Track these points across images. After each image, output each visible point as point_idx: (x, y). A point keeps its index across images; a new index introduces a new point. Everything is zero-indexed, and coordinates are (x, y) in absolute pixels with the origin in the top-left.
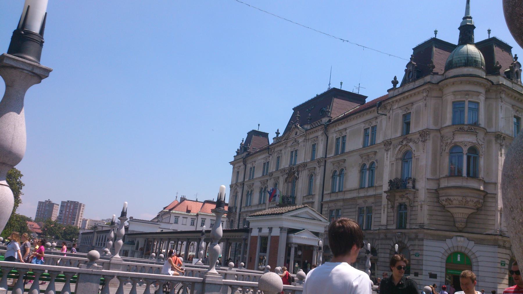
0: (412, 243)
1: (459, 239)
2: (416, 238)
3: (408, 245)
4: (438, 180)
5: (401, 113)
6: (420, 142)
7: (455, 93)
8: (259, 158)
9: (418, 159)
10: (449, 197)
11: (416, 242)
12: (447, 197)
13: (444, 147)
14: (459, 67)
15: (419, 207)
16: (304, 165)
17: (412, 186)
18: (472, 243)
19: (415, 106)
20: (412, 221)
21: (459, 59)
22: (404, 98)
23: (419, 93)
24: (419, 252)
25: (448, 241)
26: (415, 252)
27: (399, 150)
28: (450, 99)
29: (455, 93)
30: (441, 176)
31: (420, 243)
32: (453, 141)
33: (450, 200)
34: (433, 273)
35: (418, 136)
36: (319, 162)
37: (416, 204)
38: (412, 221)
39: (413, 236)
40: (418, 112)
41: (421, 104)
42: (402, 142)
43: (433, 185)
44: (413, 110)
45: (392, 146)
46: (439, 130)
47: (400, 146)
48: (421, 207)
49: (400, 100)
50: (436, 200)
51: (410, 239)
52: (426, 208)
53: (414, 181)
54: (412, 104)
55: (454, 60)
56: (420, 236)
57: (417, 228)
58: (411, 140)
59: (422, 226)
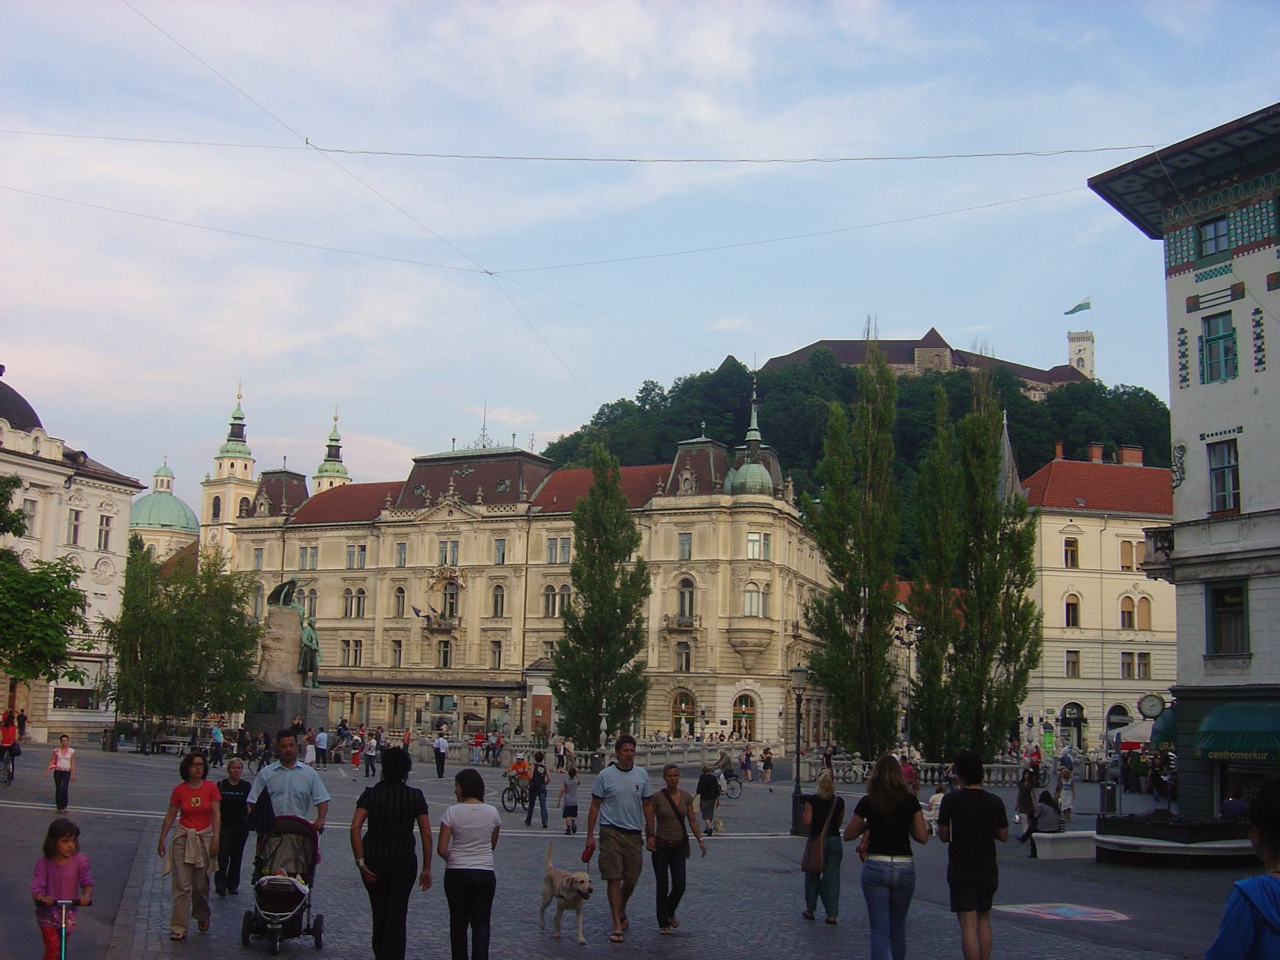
0: (699, 688)
5: (676, 531)
8: (329, 534)
11: (706, 688)
16: (479, 569)
19: (697, 527)
31: (712, 688)
36: (516, 568)
39: (700, 680)
40: (702, 536)
43: (724, 625)
44: (695, 531)
45: (661, 570)
46: (731, 562)
51: (697, 684)
54: (693, 523)
58: (693, 568)
59: (714, 670)
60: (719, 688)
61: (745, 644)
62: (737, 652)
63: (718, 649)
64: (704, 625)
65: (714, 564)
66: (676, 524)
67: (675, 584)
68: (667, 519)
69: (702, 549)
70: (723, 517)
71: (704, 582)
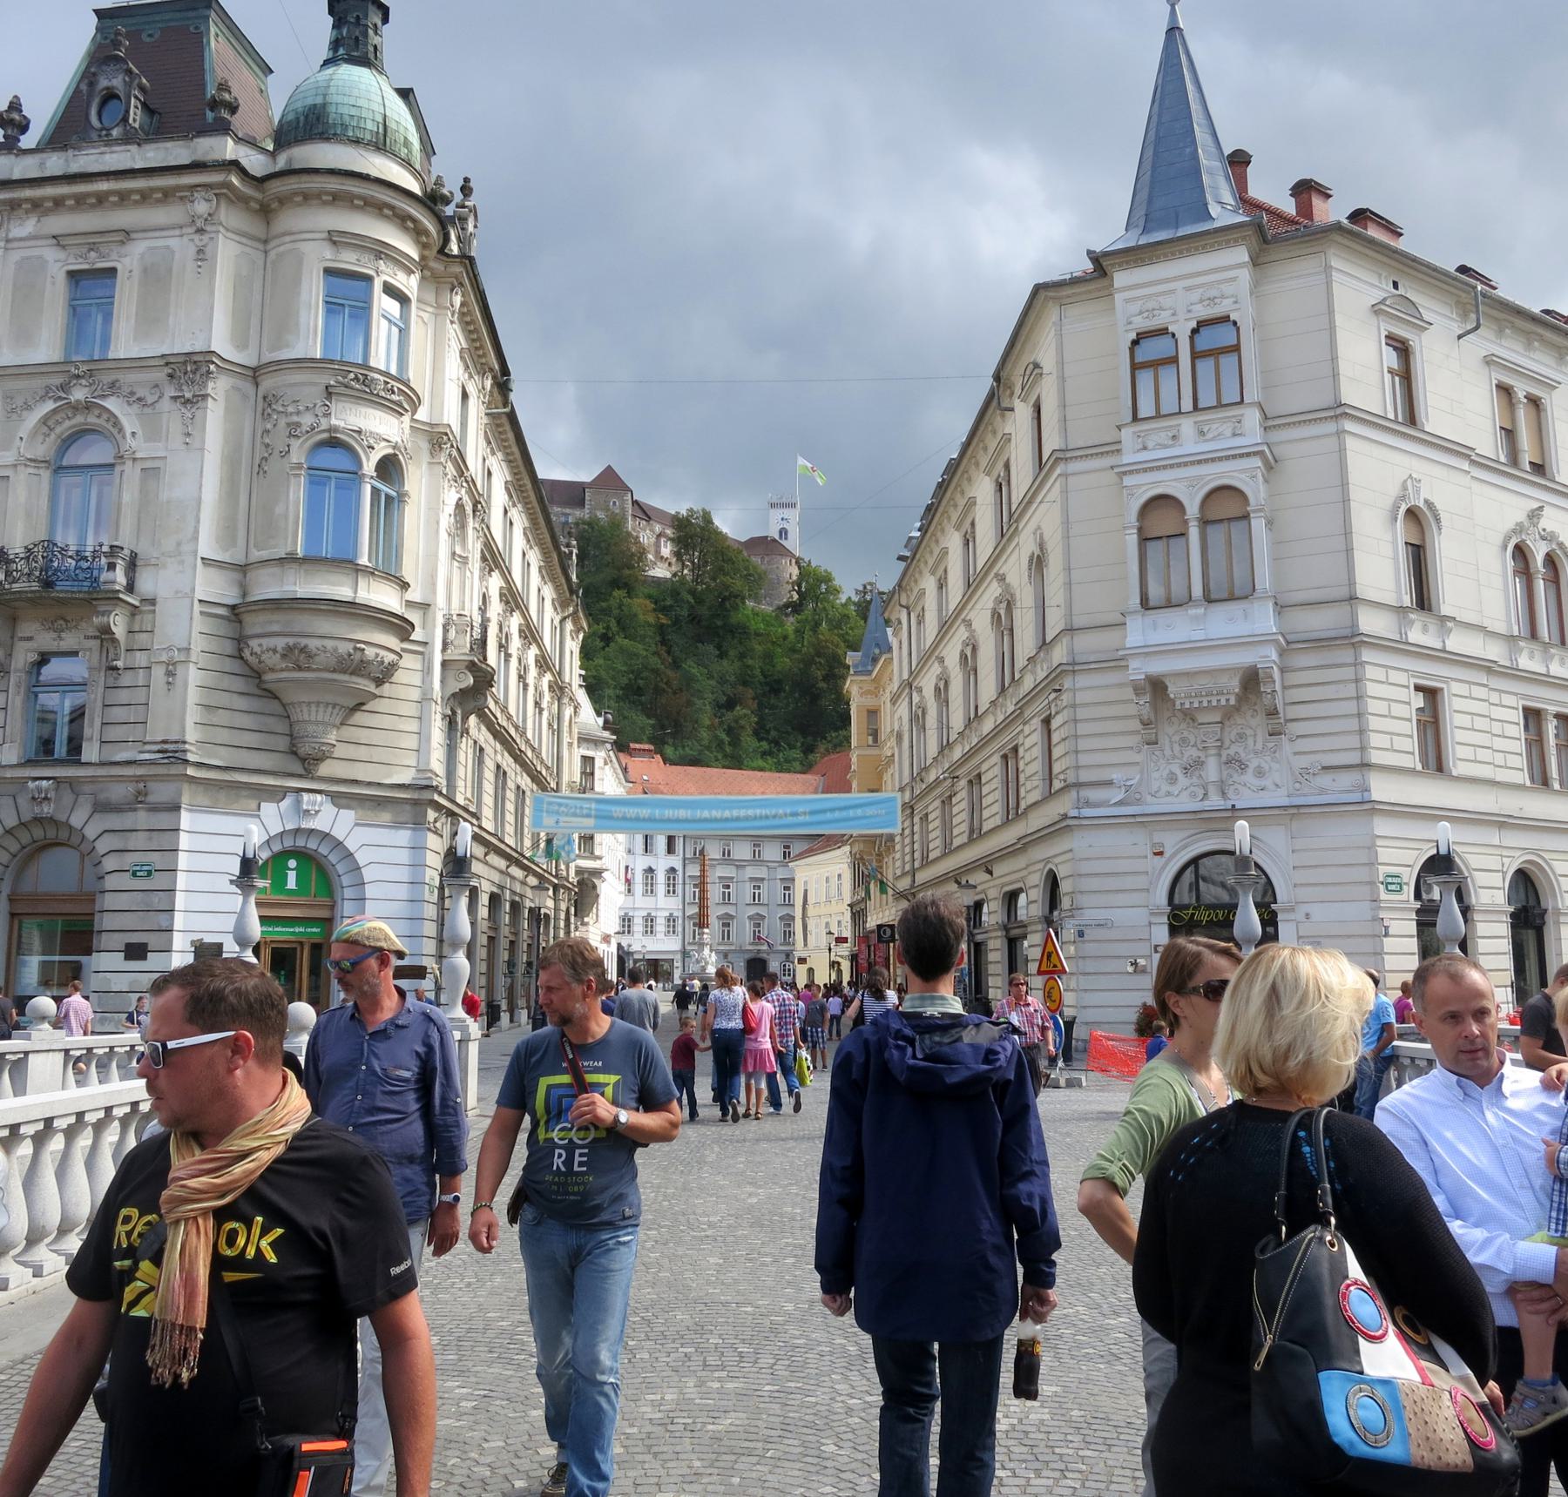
0: (114, 821)
1: (306, 796)
2: (139, 800)
3: (91, 832)
4: (243, 569)
5: (57, 263)
6: (166, 404)
7: (336, 239)
9: (152, 473)
10: (303, 641)
11: (142, 819)
12: (291, 641)
13: (279, 444)
14: (357, 142)
15: (158, 673)
17: (124, 582)
18: (348, 816)
19: (138, 248)
20: (114, 733)
21: (353, 112)
22: (80, 201)
23: (167, 195)
24: (154, 857)
25: (268, 809)
26: (129, 860)
27: (45, 421)
28: (318, 256)
29: (336, 239)
30: (256, 555)
31: (162, 820)
32: (324, 424)
33: (303, 650)
34: (209, 939)
35: (161, 375)
37: (140, 659)
38: (114, 733)
39: (119, 792)
40: (157, 277)
41: (181, 246)
42: (64, 387)
44: (129, 261)
46: (255, 374)
47: (50, 405)
48: (170, 674)
49: (58, 203)
50: (229, 647)
52: (193, 677)
53: (132, 565)
54: (126, 235)
55: (332, 109)
56: (160, 793)
57: (152, 763)
60: (186, 819)
61: (298, 656)
62: (273, 695)
63: (193, 677)
64: (147, 583)
65: (189, 371)
66: (57, 240)
67: (43, 449)
68: (25, 227)
69: (150, 319)
70: (230, 217)
71: (153, 435)
